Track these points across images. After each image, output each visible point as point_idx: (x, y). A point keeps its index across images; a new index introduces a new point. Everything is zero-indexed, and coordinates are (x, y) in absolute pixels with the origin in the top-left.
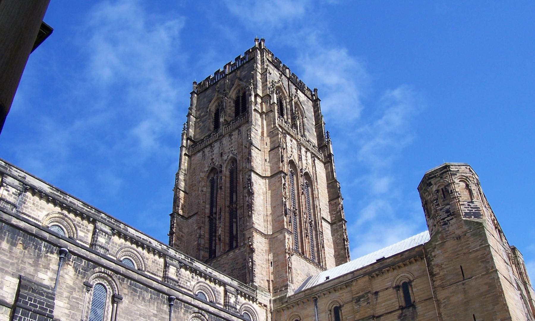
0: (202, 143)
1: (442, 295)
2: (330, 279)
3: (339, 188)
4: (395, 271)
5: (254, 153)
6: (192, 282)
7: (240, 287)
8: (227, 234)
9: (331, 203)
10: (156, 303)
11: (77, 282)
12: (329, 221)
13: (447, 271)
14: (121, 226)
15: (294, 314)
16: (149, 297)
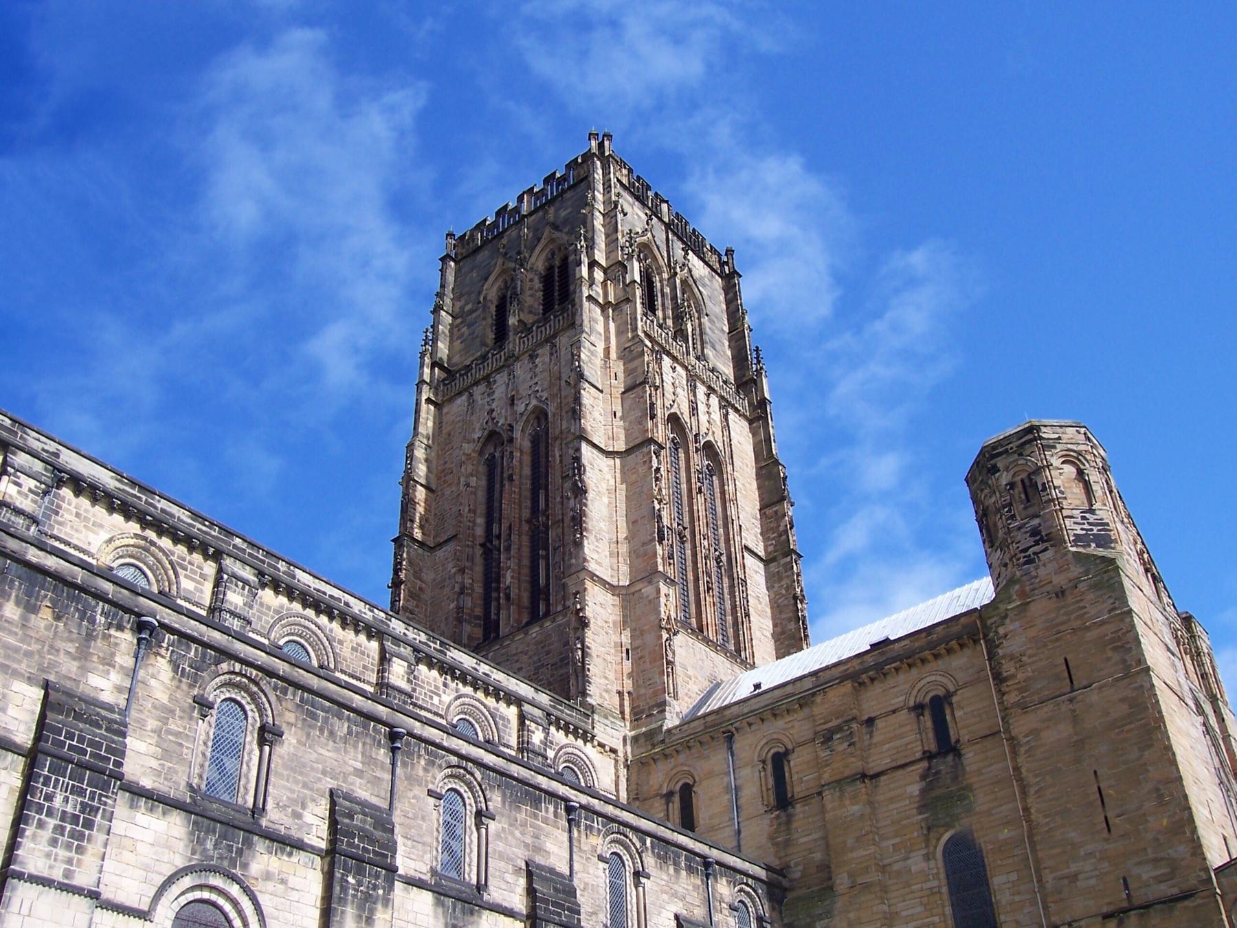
0: (466, 374)
1: (1021, 725)
2: (764, 688)
3: (785, 478)
4: (914, 671)
5: (588, 396)
6: (443, 695)
7: (554, 707)
8: (525, 585)
9: (765, 513)
10: (360, 745)
11: (178, 695)
12: (762, 554)
13: (1033, 671)
14: (279, 566)
15: (679, 769)
16: (345, 730)
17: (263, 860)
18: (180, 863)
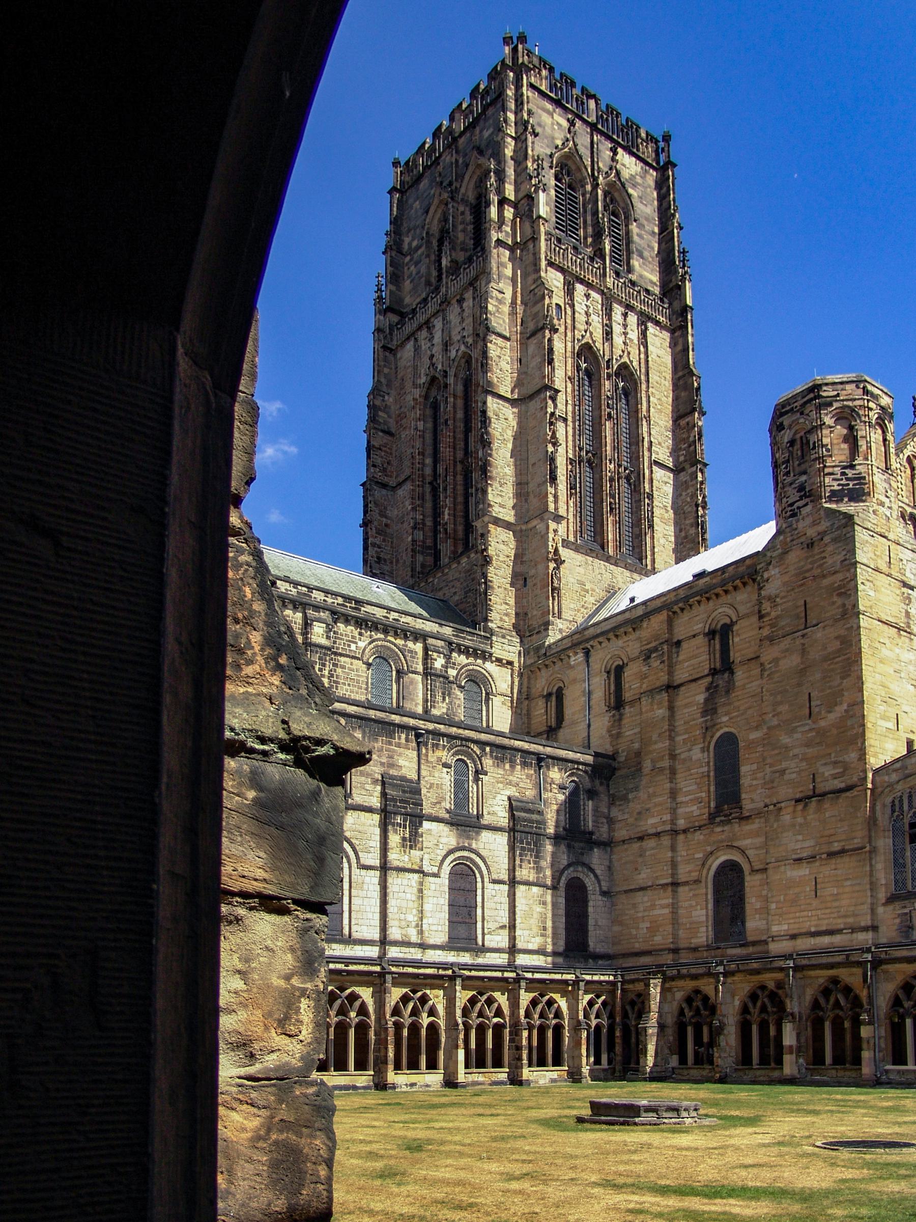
0: (413, 318)
3: (698, 389)
7: (457, 636)
8: (460, 520)
12: (671, 465)
13: (782, 611)
15: (554, 676)
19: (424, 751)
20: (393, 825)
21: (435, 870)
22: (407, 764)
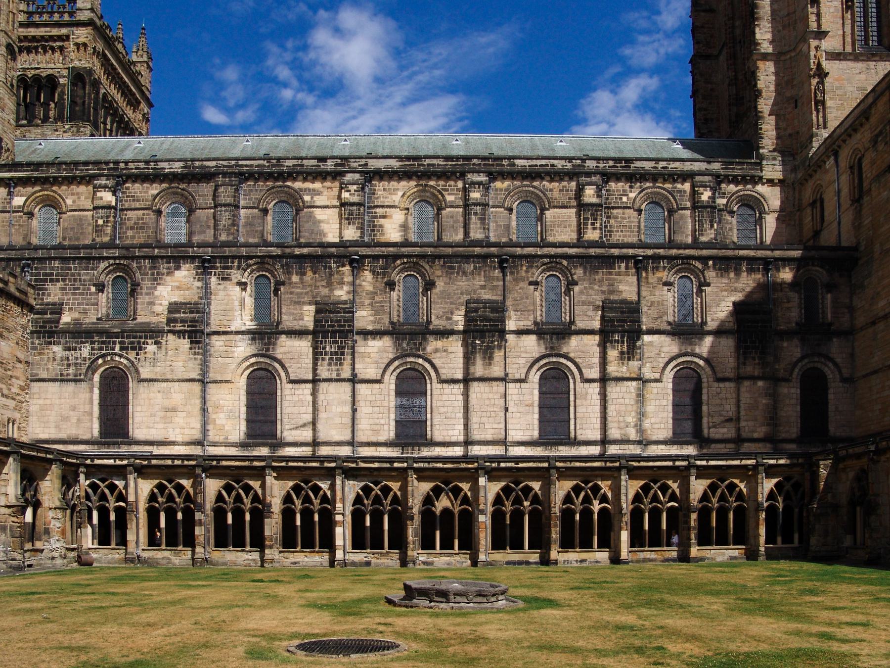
16: (472, 268)
17: (433, 345)
18: (391, 356)
19: (644, 275)
20: (611, 342)
21: (657, 376)
22: (627, 288)
